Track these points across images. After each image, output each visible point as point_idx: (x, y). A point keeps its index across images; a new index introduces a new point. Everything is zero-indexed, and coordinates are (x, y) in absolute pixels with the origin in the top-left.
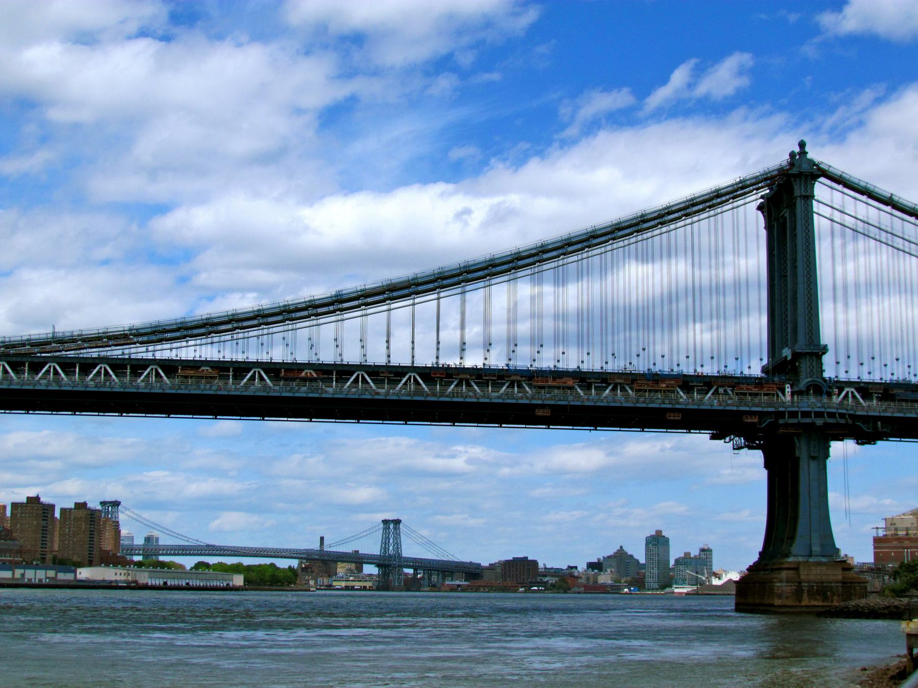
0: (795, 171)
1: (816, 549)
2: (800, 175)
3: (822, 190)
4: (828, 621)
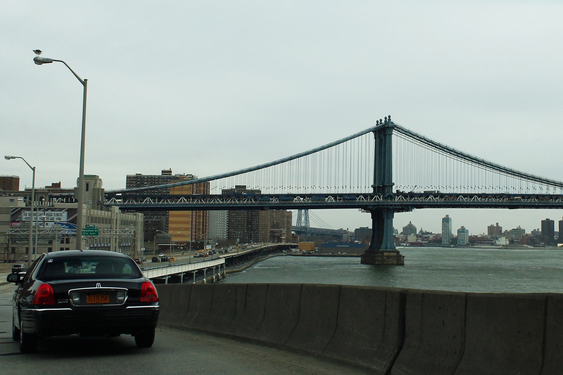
0: (386, 126)
1: (389, 246)
2: (388, 127)
3: (394, 132)
4: (397, 267)
